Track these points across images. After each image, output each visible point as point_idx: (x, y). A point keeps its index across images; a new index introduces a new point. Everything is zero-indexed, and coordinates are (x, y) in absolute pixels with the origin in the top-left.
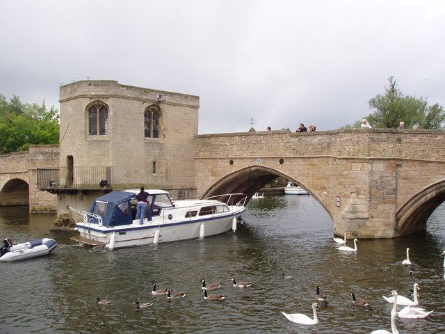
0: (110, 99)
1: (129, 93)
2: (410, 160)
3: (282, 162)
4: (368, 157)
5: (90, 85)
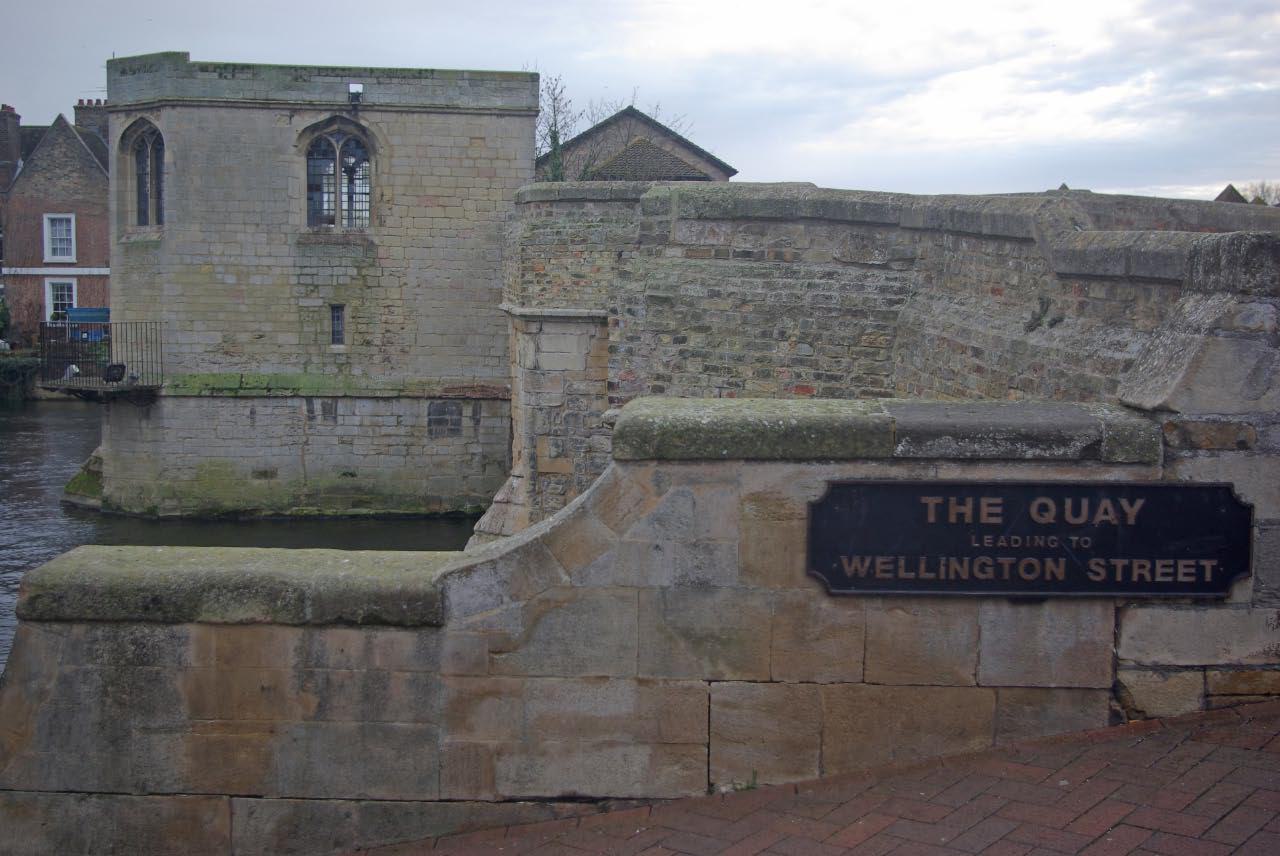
0: (166, 113)
1: (227, 90)
5: (123, 72)
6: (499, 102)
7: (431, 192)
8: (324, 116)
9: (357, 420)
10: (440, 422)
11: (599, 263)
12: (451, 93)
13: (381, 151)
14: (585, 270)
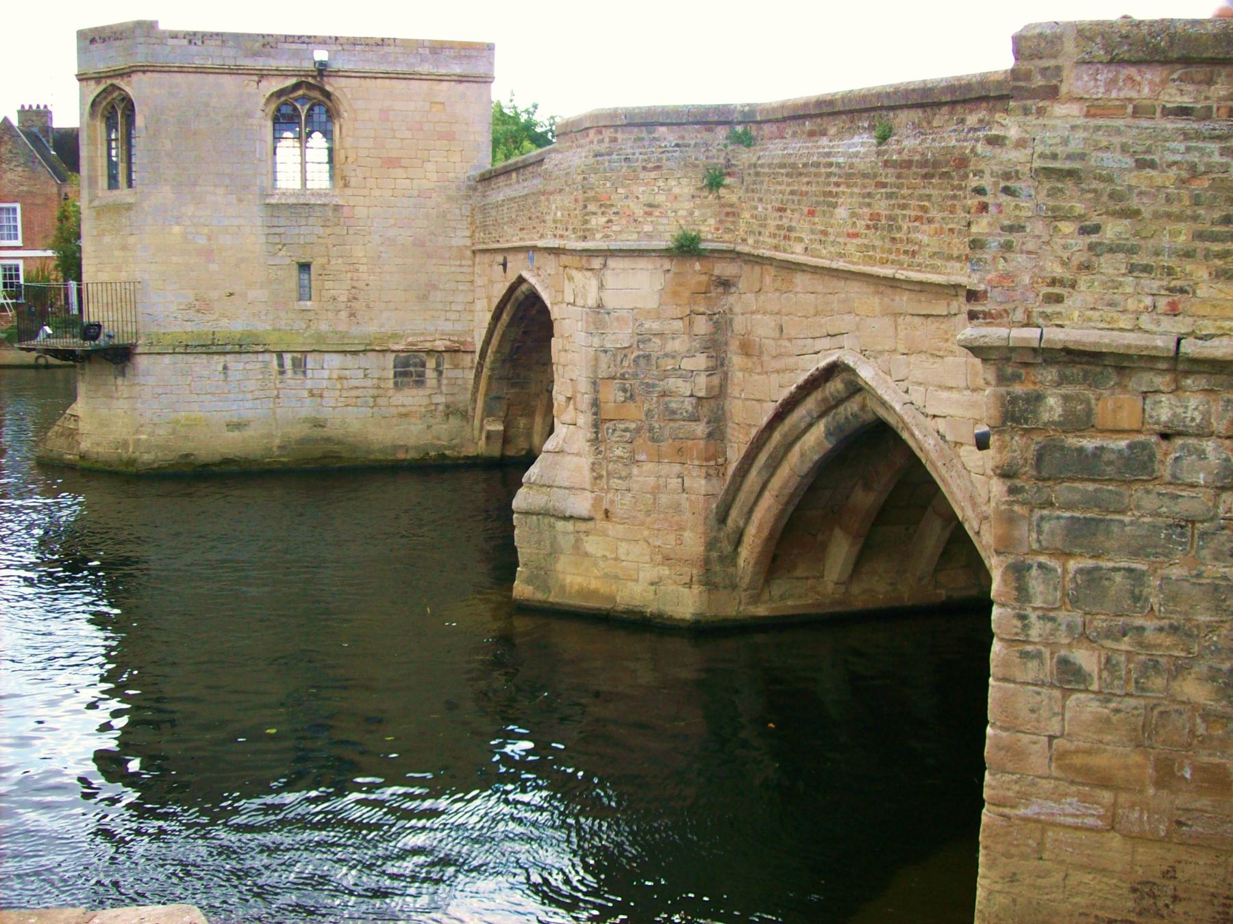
6: (458, 70)
7: (394, 154)
8: (292, 81)
9: (326, 374)
10: (406, 374)
11: (676, 190)
12: (413, 60)
13: (345, 115)
14: (661, 198)
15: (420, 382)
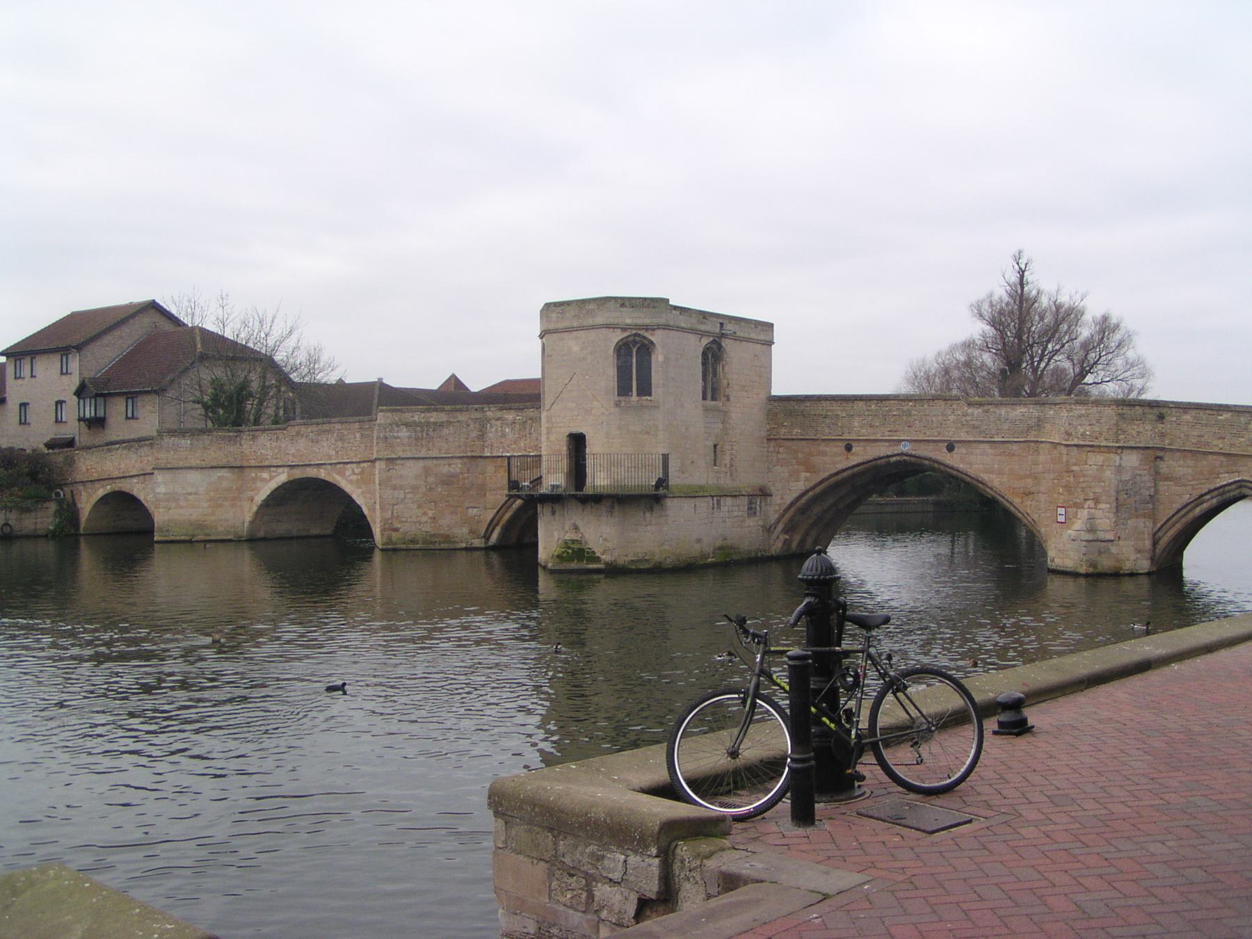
0: (659, 332)
1: (683, 322)
2: (1178, 450)
3: (950, 448)
4: (1114, 444)
5: (623, 305)
15: (755, 513)
